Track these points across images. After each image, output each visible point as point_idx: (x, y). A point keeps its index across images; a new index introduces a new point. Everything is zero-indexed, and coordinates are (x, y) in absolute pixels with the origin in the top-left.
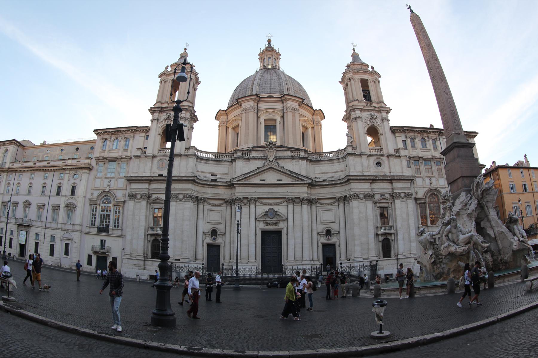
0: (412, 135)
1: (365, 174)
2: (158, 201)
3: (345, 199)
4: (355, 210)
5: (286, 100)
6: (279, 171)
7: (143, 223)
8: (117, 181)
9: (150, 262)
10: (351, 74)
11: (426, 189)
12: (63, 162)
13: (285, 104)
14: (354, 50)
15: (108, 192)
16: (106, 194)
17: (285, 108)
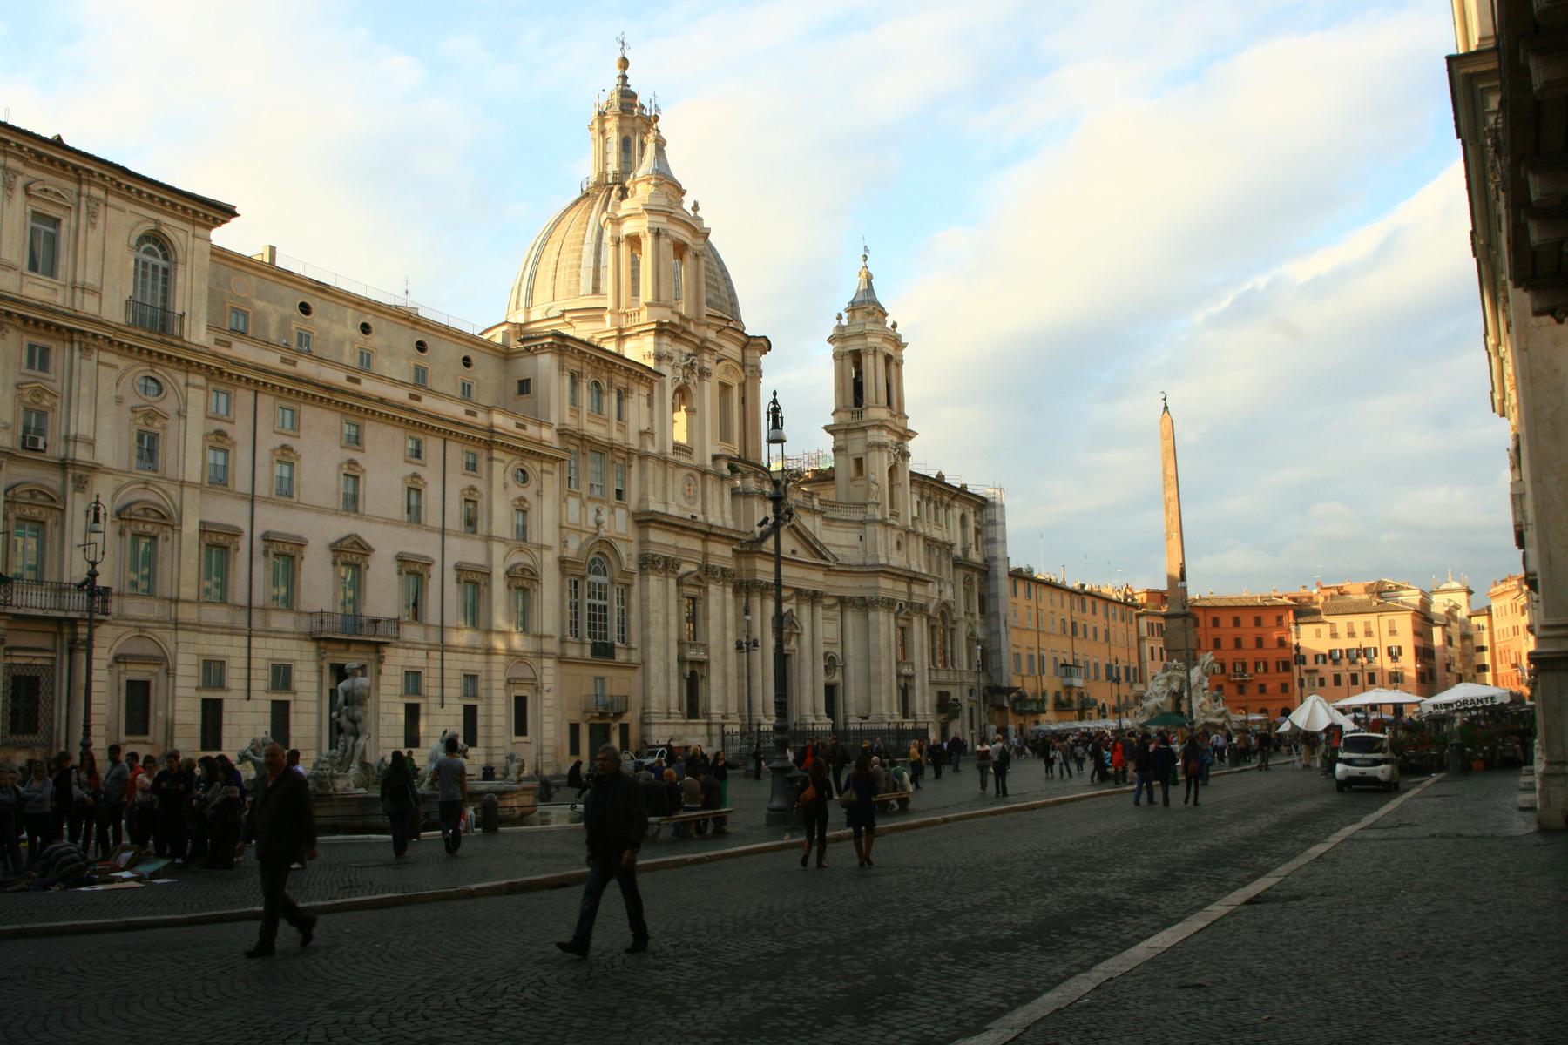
0: (927, 492)
1: (893, 563)
2: (693, 581)
3: (865, 605)
4: (883, 629)
5: (754, 347)
6: (797, 531)
7: (674, 635)
8: (613, 512)
9: (691, 726)
10: (879, 340)
11: (935, 601)
12: (350, 379)
13: (748, 353)
14: (865, 258)
15: (606, 542)
16: (603, 550)
17: (749, 361)
